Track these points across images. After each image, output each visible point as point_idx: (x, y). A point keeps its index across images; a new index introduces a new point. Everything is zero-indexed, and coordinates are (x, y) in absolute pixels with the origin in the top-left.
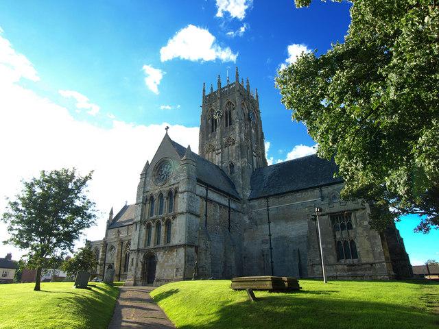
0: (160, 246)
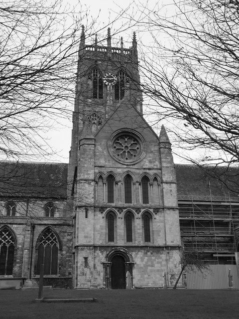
0: (134, 245)
